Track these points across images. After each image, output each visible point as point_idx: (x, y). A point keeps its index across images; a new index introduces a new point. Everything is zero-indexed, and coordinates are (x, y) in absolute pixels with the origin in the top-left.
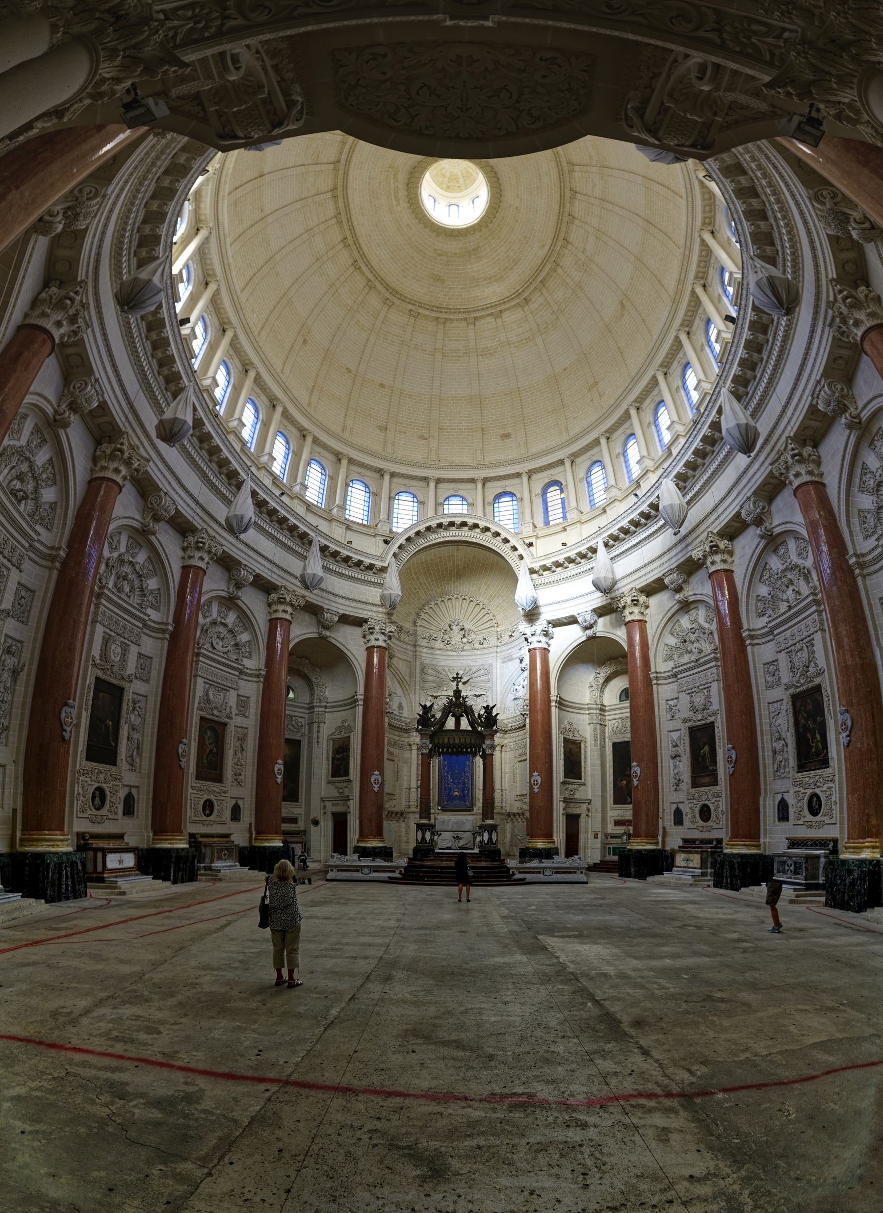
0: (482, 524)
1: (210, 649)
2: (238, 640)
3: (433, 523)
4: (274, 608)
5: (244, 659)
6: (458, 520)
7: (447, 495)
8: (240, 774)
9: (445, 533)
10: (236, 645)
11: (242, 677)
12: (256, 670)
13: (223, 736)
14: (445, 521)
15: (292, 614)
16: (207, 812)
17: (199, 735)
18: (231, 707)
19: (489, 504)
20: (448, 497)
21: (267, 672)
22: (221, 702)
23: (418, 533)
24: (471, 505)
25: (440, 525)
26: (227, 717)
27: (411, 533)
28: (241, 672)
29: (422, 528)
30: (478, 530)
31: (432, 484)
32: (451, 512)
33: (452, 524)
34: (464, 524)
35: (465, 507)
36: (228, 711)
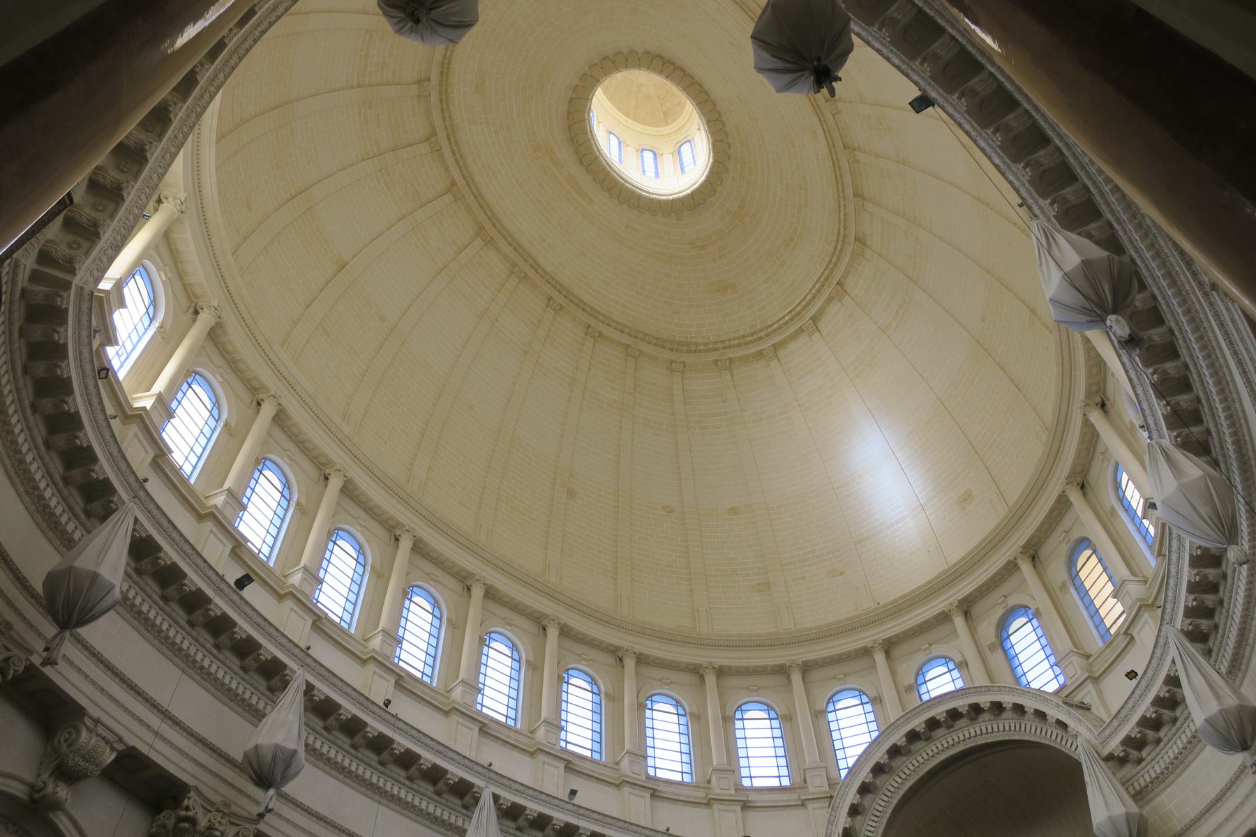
0: (984, 700)
3: (898, 737)
6: (939, 712)
7: (917, 666)
9: (933, 748)
14: (917, 723)
19: (992, 648)
20: (921, 669)
23: (878, 769)
24: (962, 666)
25: (913, 736)
27: (864, 775)
29: (880, 755)
30: (986, 716)
31: (879, 657)
32: (933, 694)
33: (933, 724)
34: (954, 715)
35: (956, 673)
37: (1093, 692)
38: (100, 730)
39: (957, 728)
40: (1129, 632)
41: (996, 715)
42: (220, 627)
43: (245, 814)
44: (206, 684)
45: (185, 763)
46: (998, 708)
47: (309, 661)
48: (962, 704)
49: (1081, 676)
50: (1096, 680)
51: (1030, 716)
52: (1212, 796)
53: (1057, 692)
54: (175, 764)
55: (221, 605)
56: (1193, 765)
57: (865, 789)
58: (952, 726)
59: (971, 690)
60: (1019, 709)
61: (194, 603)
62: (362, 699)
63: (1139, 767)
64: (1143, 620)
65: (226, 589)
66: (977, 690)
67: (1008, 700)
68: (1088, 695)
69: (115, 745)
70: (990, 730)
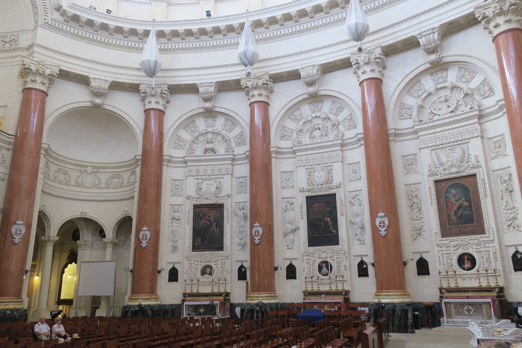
1: (436, 118)
18: (476, 157)
22: (459, 158)
38: (204, 85)
42: (217, 31)
43: (262, 74)
44: (232, 47)
45: (237, 74)
47: (252, 14)
54: (234, 76)
55: (208, 26)
61: (203, 32)
62: (281, 7)
65: (207, 21)
69: (211, 85)
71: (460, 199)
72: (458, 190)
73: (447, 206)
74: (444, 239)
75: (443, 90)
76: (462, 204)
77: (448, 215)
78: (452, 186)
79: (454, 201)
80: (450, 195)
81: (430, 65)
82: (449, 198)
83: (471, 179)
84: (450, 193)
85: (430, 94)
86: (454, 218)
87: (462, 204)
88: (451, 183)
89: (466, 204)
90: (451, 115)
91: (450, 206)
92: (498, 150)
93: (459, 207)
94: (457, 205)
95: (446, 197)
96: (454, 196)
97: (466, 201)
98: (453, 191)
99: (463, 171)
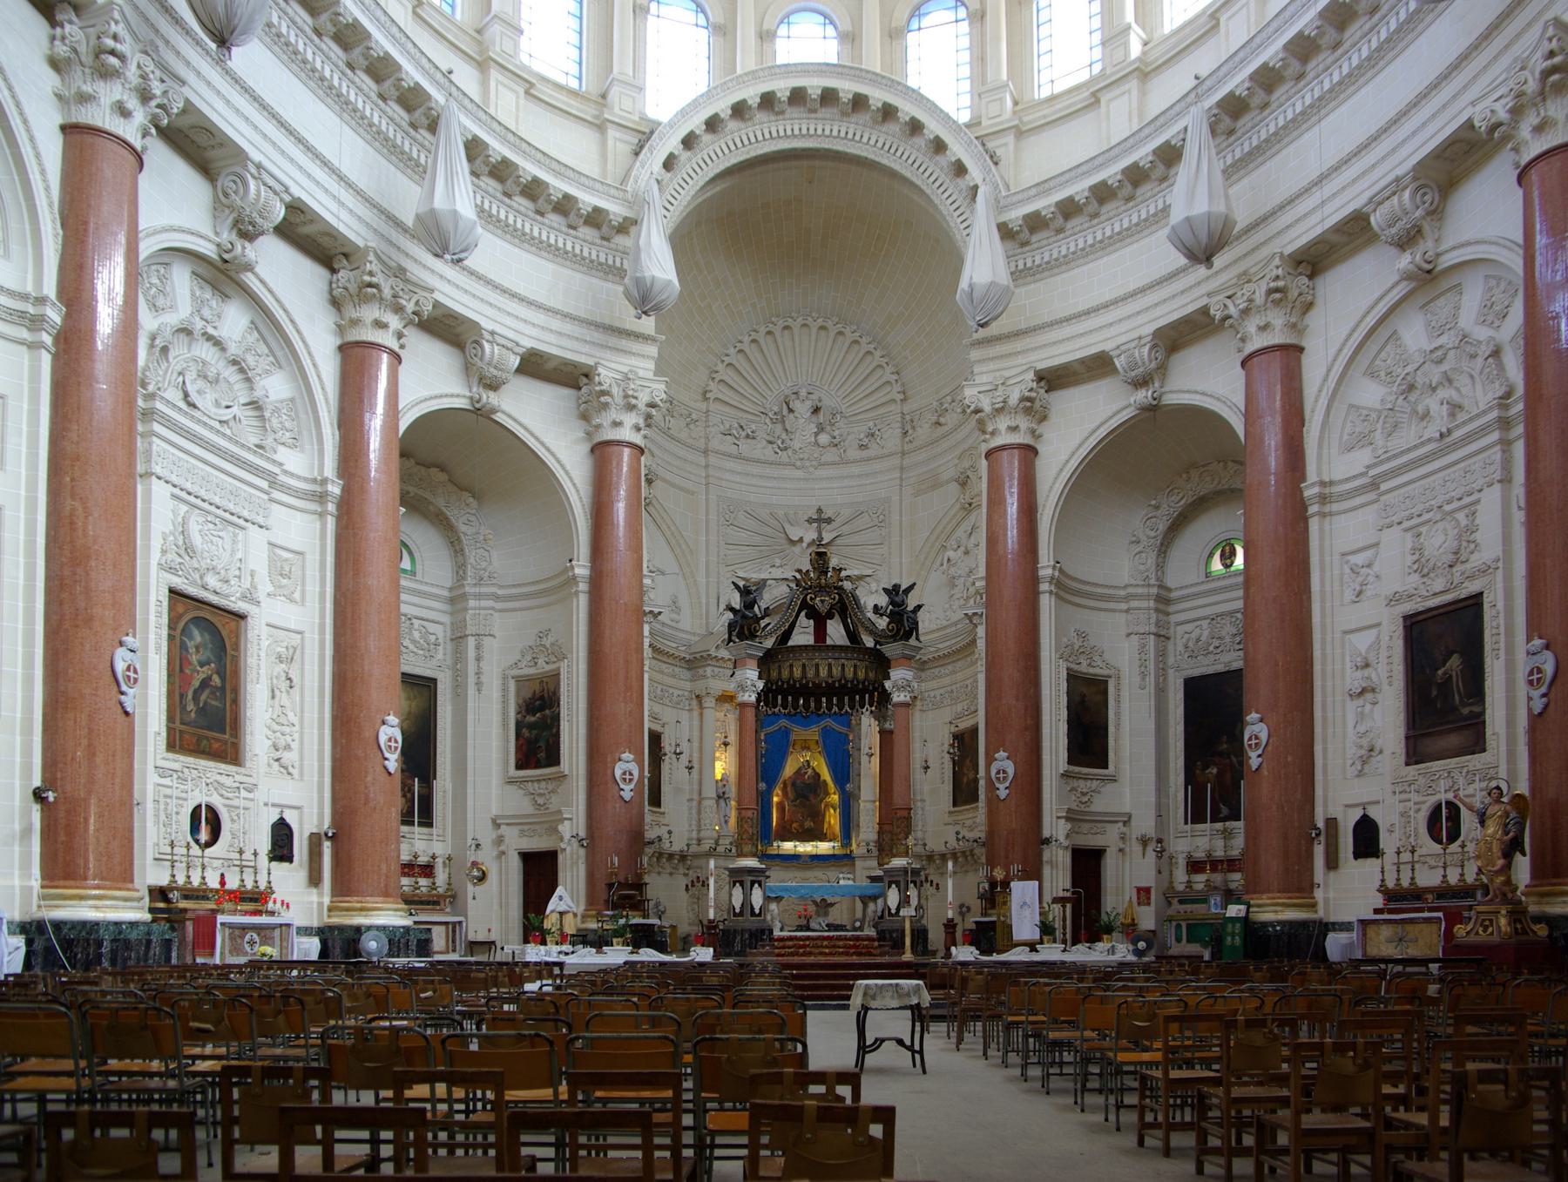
0: (877, 96)
2: (258, 393)
3: (751, 94)
4: (351, 312)
5: (281, 448)
8: (288, 747)
10: (255, 405)
11: (277, 495)
12: (314, 481)
13: (236, 647)
15: (400, 336)
16: (204, 836)
17: (171, 638)
21: (346, 490)
23: (713, 124)
26: (244, 598)
28: (273, 483)
29: (722, 106)
30: (863, 118)
36: (246, 584)
37: (1011, 147)
39: (819, 115)
40: (1099, 95)
41: (875, 122)
46: (888, 112)
48: (847, 87)
49: (1008, 121)
50: (1020, 133)
51: (919, 141)
52: (1081, 308)
53: (968, 126)
56: (1076, 271)
57: (689, 142)
58: (815, 111)
59: (869, 76)
60: (915, 127)
63: (1019, 251)
64: (1127, 87)
66: (874, 79)
67: (907, 110)
68: (1005, 147)
70: (857, 138)
71: (208, 663)
72: (207, 636)
73: (182, 671)
74: (170, 755)
75: (216, 348)
76: (209, 678)
77: (182, 696)
78: (197, 621)
79: (196, 663)
80: (190, 644)
81: (215, 256)
82: (187, 650)
83: (233, 624)
84: (191, 638)
85: (217, 343)
86: (191, 707)
87: (209, 678)
88: (202, 614)
89: (216, 680)
90: (217, 425)
91: (187, 671)
92: (285, 581)
93: (205, 683)
94: (202, 676)
95: (183, 646)
96: (197, 648)
97: (218, 673)
98: (198, 637)
99: (227, 596)
